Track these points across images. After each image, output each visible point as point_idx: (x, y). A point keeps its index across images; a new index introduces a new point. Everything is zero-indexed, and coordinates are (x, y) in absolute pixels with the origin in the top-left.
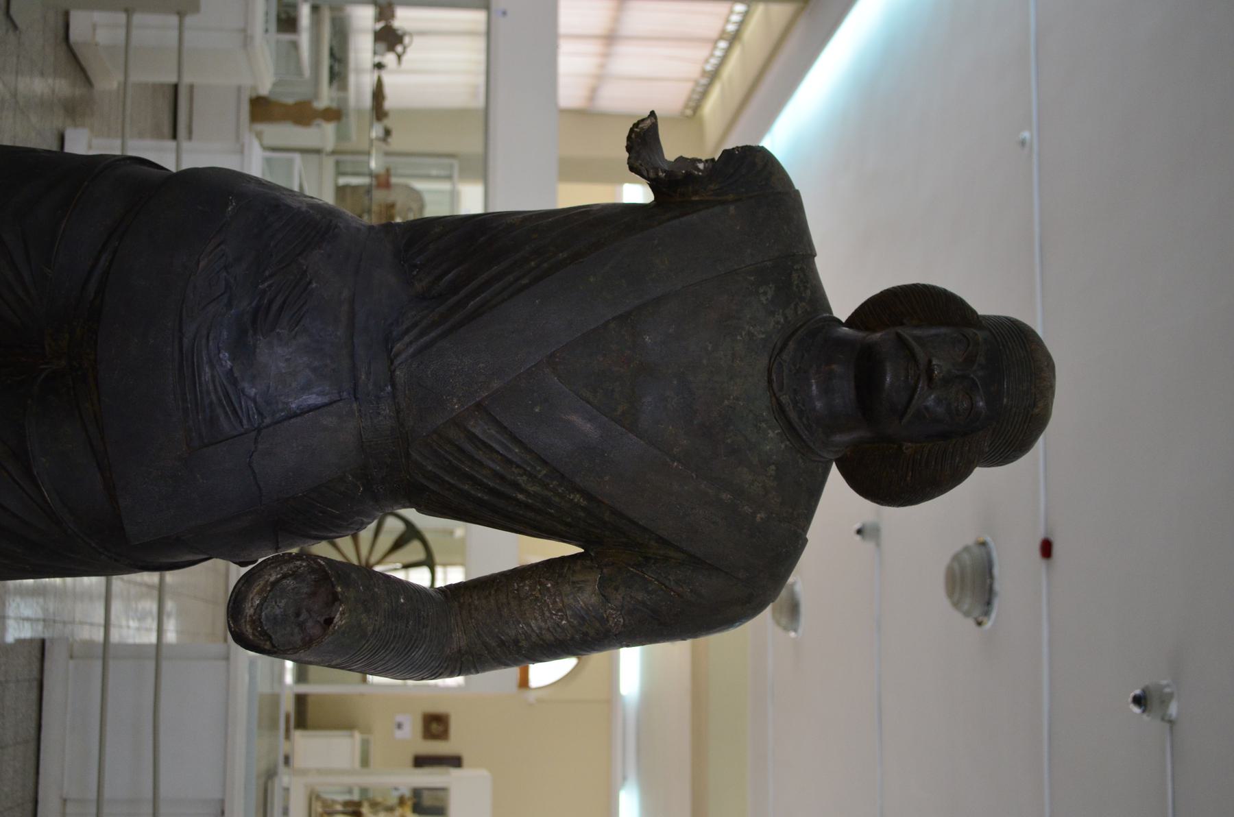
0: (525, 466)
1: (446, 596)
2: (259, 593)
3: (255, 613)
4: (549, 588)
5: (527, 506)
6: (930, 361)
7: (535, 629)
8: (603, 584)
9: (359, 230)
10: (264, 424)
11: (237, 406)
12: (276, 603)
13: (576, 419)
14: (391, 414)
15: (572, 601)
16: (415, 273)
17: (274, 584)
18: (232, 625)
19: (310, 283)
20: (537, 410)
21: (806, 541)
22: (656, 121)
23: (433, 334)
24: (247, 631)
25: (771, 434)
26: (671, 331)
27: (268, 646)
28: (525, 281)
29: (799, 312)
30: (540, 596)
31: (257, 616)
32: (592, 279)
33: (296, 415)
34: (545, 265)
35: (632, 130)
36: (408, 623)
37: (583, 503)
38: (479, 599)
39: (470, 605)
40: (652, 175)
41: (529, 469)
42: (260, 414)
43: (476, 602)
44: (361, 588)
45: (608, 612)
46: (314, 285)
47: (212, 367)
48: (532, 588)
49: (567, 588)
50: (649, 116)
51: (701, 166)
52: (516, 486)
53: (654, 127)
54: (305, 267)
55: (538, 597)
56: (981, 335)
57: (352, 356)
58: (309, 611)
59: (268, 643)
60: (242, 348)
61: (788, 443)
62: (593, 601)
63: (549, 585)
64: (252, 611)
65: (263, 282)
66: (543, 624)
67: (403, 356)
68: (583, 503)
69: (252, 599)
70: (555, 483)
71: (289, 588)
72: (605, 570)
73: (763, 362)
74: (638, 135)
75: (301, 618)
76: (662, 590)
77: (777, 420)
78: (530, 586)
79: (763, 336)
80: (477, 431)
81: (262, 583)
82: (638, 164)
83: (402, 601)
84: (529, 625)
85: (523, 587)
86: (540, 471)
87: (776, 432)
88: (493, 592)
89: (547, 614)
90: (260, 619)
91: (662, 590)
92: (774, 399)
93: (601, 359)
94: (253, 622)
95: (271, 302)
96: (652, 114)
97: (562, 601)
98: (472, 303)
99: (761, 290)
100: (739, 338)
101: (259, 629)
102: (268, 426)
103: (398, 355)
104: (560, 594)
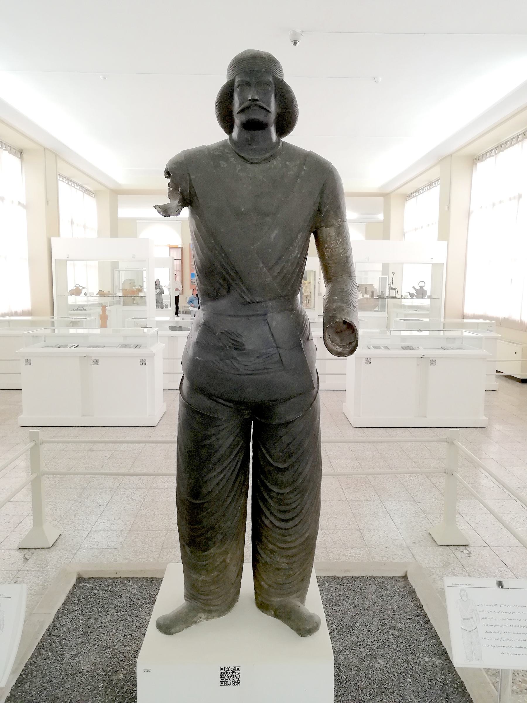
6: (250, 100)
7: (343, 250)
8: (327, 226)
9: (204, 314)
13: (273, 236)
17: (332, 342)
25: (275, 163)
27: (354, 344)
28: (223, 255)
29: (229, 152)
36: (344, 295)
40: (180, 207)
42: (271, 347)
48: (328, 251)
49: (328, 239)
51: (171, 189)
53: (160, 207)
56: (237, 79)
57: (251, 316)
61: (278, 157)
64: (341, 349)
73: (249, 166)
75: (339, 331)
83: (336, 297)
88: (329, 265)
89: (337, 246)
92: (263, 162)
94: (345, 348)
95: (233, 344)
96: (154, 207)
98: (232, 274)
99: (222, 166)
102: (276, 344)
103: (251, 300)
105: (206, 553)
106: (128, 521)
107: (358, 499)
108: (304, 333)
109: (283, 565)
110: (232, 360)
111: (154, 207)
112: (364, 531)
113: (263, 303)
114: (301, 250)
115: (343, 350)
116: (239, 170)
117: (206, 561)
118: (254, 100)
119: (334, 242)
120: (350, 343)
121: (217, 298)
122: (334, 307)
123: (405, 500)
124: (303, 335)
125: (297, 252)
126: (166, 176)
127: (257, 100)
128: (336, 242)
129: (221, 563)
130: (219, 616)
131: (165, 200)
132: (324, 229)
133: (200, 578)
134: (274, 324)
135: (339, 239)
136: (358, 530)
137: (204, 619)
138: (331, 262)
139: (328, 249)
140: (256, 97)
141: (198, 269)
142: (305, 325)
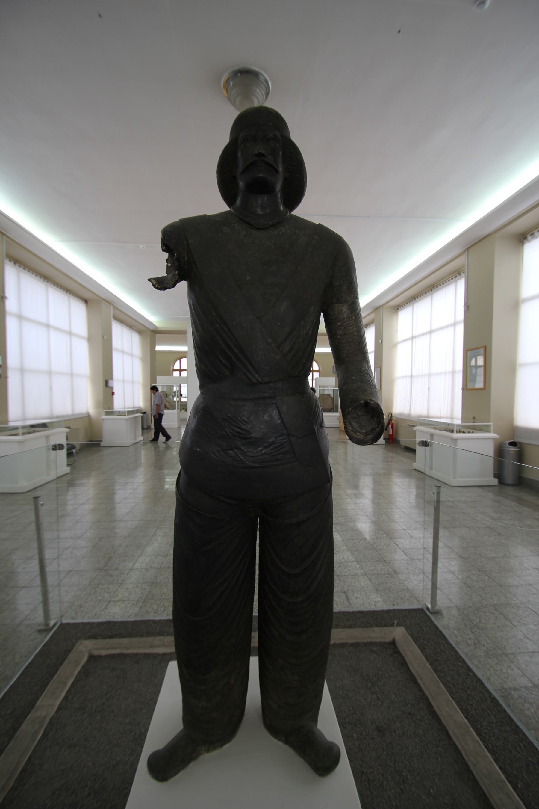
3: (363, 435)
6: (256, 155)
7: (356, 328)
8: (339, 302)
9: (204, 398)
11: (279, 444)
12: (354, 426)
16: (221, 375)
18: (369, 443)
19: (229, 417)
21: (319, 224)
22: (151, 278)
23: (249, 367)
24: (370, 437)
25: (284, 230)
28: (226, 329)
30: (344, 327)
33: (283, 421)
35: (157, 288)
43: (346, 351)
44: (356, 393)
45: (350, 301)
46: (229, 415)
50: (150, 281)
51: (169, 265)
53: (154, 279)
54: (222, 419)
55: (344, 328)
59: (376, 429)
63: (339, 324)
67: (259, 379)
69: (357, 436)
72: (334, 302)
74: (159, 285)
75: (356, 416)
77: (278, 228)
81: (351, 432)
82: (173, 282)
83: (354, 378)
84: (355, 331)
87: (282, 228)
88: (342, 345)
89: (351, 324)
94: (366, 435)
95: (238, 432)
96: (149, 280)
97: (346, 318)
98: (236, 351)
100: (246, 241)
101: (370, 433)
103: (258, 381)
106: (144, 589)
107: (339, 561)
108: (317, 418)
110: (237, 451)
111: (149, 280)
112: (348, 593)
113: (271, 384)
118: (260, 155)
120: (373, 430)
122: (354, 387)
123: (377, 561)
124: (316, 421)
125: (308, 328)
126: (164, 248)
127: (263, 155)
131: (162, 273)
135: (353, 317)
136: (343, 592)
139: (340, 327)
140: (263, 152)
141: (197, 348)
142: (317, 409)
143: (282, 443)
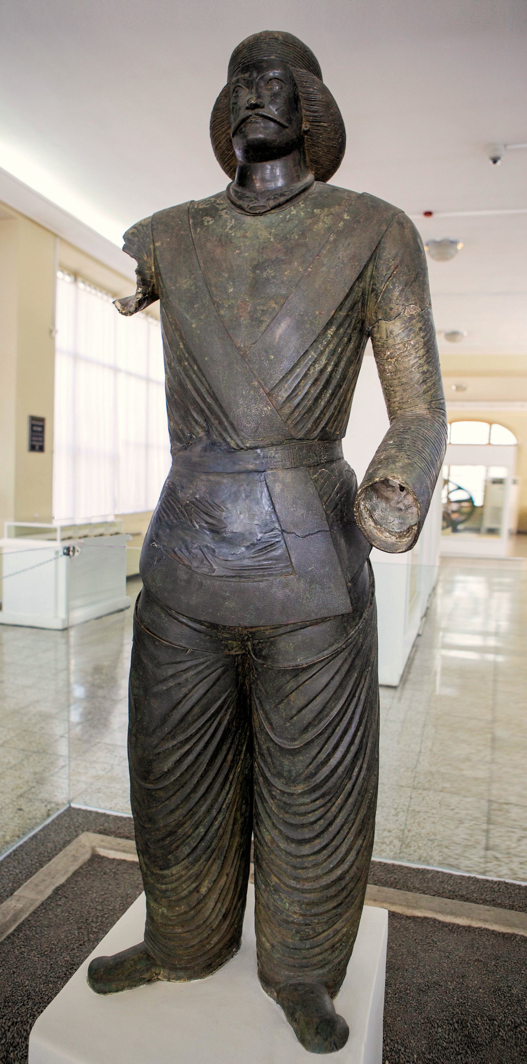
0: (309, 365)
1: (394, 418)
2: (382, 533)
4: (391, 353)
5: (336, 365)
7: (416, 361)
8: (387, 318)
10: (279, 528)
14: (274, 449)
15: (399, 338)
18: (401, 550)
19: (196, 499)
20: (273, 357)
23: (226, 423)
26: (226, 276)
28: (196, 368)
31: (397, 535)
32: (194, 326)
33: (274, 508)
34: (187, 355)
36: (406, 438)
37: (333, 329)
38: (396, 397)
39: (399, 403)
41: (310, 363)
42: (272, 530)
43: (398, 399)
46: (197, 496)
47: (244, 558)
49: (390, 341)
52: (322, 371)
58: (398, 503)
59: (414, 528)
60: (232, 541)
61: (300, 203)
62: (399, 324)
64: (393, 538)
65: (195, 527)
66: (413, 356)
68: (333, 329)
70: (320, 346)
71: (381, 514)
72: (380, 318)
73: (249, 220)
75: (403, 508)
76: (392, 279)
78: (389, 365)
79: (233, 220)
80: (285, 395)
81: (375, 531)
83: (392, 442)
84: (413, 365)
85: (389, 369)
86: (312, 356)
88: (392, 389)
89: (406, 353)
90: (399, 533)
91: (392, 279)
92: (272, 211)
93: (243, 318)
94: (400, 537)
95: (207, 523)
98: (208, 400)
99: (206, 224)
102: (280, 526)
103: (238, 445)
104: (394, 345)
105: (166, 872)
109: (295, 916)
113: (259, 451)
114: (335, 358)
115: (398, 540)
116: (232, 227)
117: (166, 884)
119: (401, 345)
121: (191, 444)
128: (404, 345)
129: (191, 893)
130: (190, 978)
132: (383, 324)
133: (160, 910)
134: (277, 488)
137: (165, 977)
138: (396, 382)
143: (270, 543)
